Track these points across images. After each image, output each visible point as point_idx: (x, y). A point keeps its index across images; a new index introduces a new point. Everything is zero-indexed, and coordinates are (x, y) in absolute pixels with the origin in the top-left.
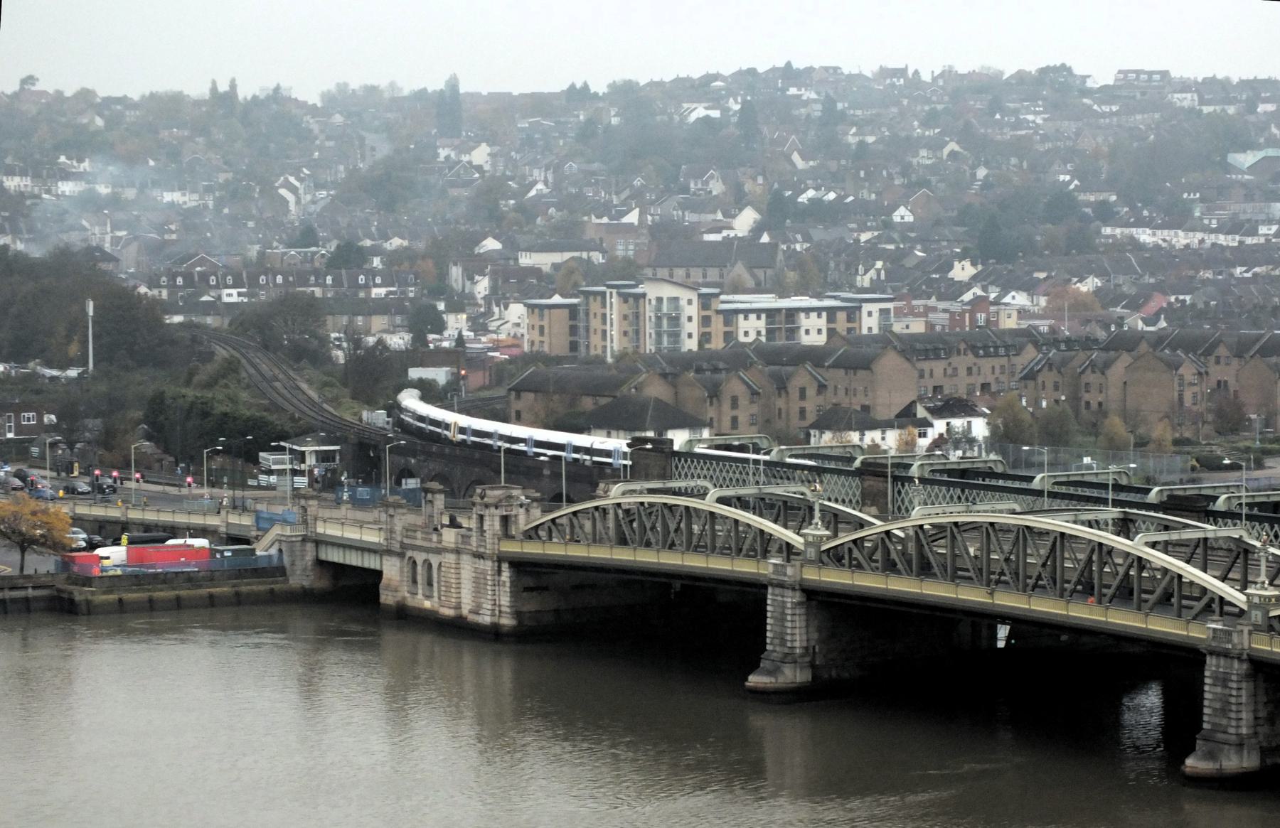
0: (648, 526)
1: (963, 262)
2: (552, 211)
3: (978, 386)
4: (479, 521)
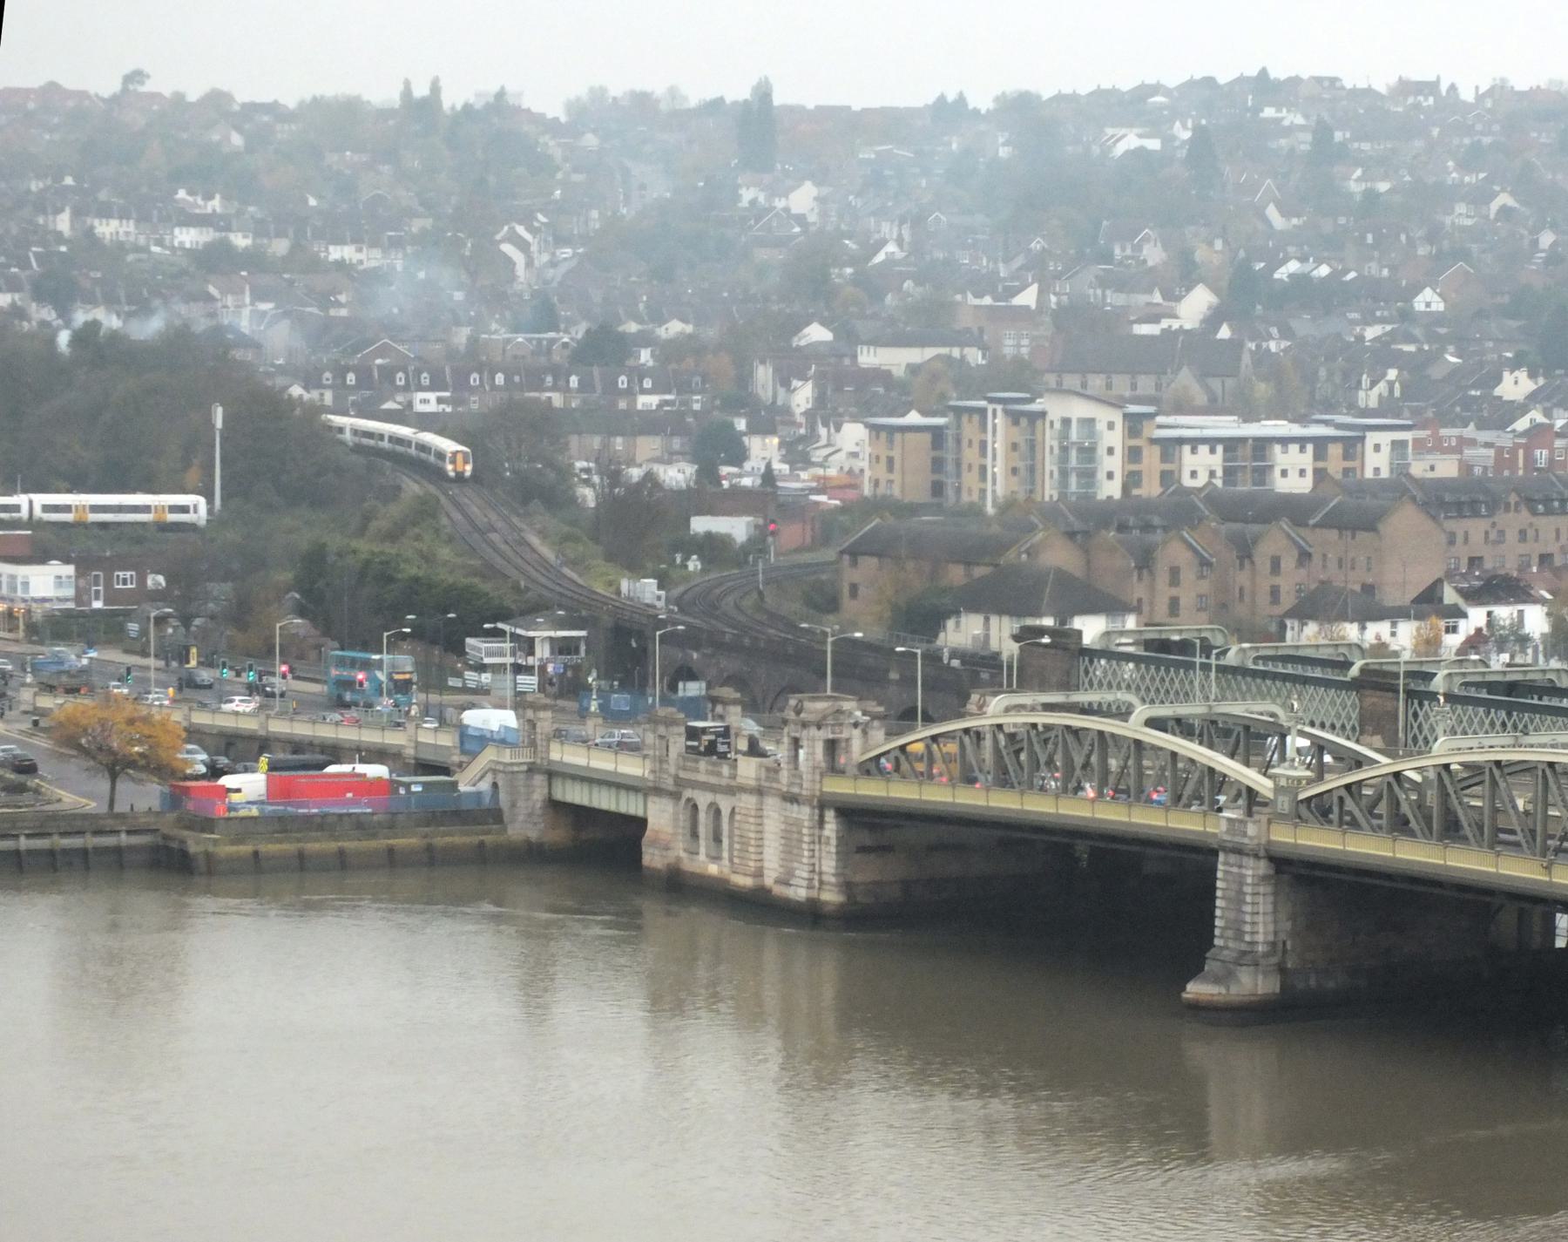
0: (1043, 759)
1: (1517, 373)
2: (908, 285)
3: (1535, 560)
4: (792, 747)
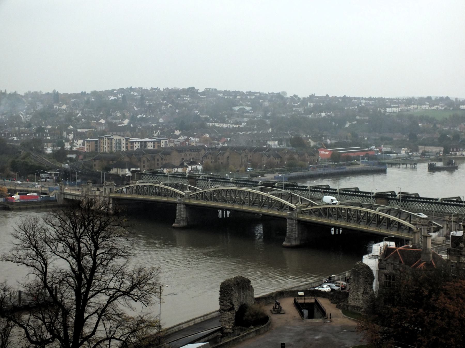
2: (83, 120)
